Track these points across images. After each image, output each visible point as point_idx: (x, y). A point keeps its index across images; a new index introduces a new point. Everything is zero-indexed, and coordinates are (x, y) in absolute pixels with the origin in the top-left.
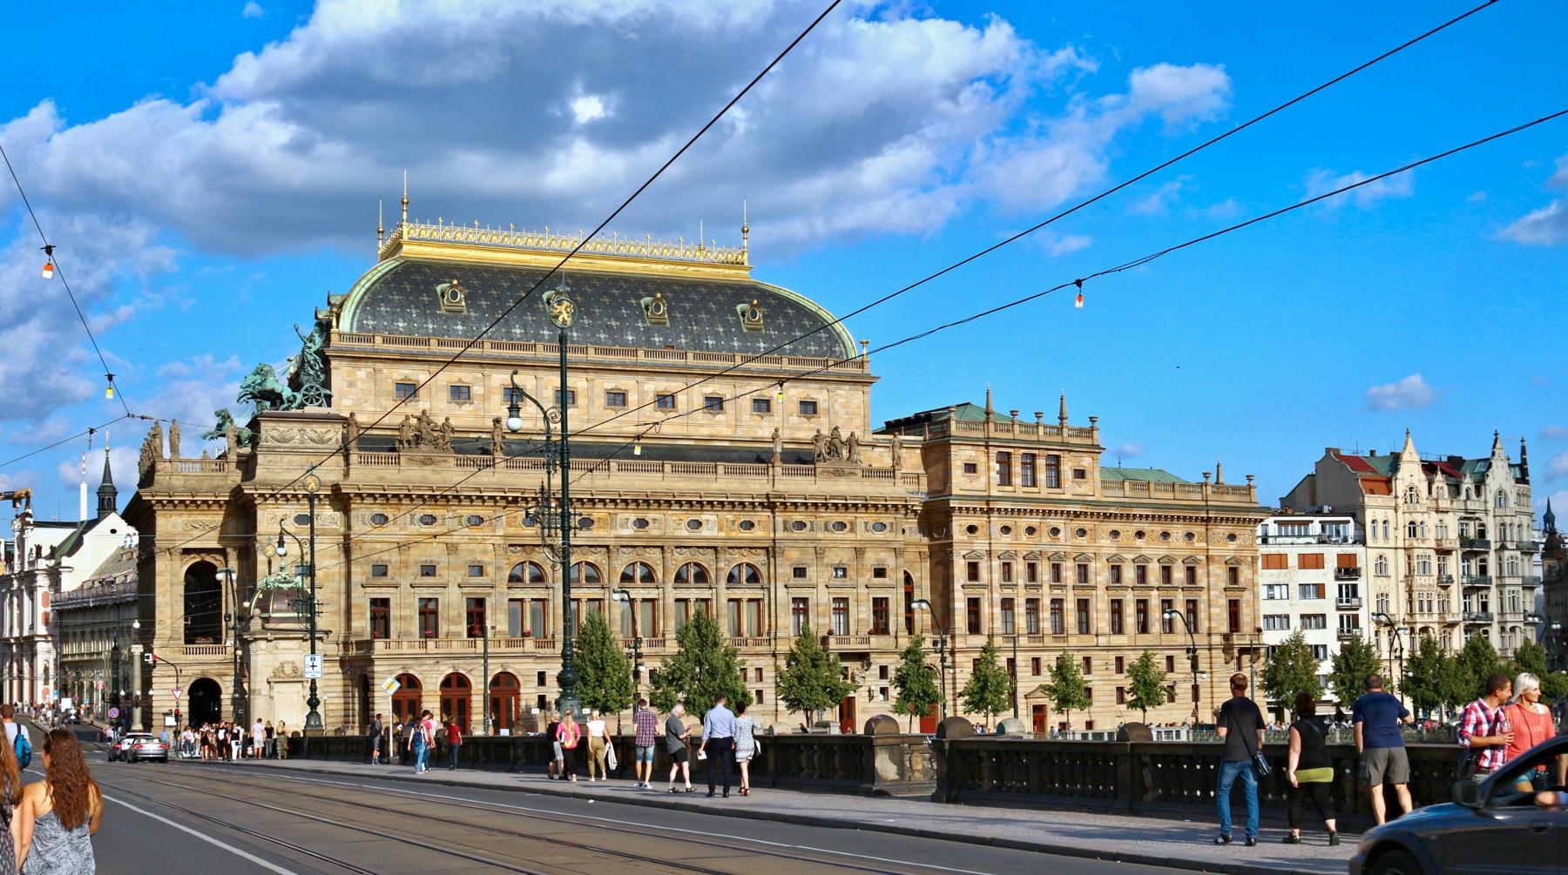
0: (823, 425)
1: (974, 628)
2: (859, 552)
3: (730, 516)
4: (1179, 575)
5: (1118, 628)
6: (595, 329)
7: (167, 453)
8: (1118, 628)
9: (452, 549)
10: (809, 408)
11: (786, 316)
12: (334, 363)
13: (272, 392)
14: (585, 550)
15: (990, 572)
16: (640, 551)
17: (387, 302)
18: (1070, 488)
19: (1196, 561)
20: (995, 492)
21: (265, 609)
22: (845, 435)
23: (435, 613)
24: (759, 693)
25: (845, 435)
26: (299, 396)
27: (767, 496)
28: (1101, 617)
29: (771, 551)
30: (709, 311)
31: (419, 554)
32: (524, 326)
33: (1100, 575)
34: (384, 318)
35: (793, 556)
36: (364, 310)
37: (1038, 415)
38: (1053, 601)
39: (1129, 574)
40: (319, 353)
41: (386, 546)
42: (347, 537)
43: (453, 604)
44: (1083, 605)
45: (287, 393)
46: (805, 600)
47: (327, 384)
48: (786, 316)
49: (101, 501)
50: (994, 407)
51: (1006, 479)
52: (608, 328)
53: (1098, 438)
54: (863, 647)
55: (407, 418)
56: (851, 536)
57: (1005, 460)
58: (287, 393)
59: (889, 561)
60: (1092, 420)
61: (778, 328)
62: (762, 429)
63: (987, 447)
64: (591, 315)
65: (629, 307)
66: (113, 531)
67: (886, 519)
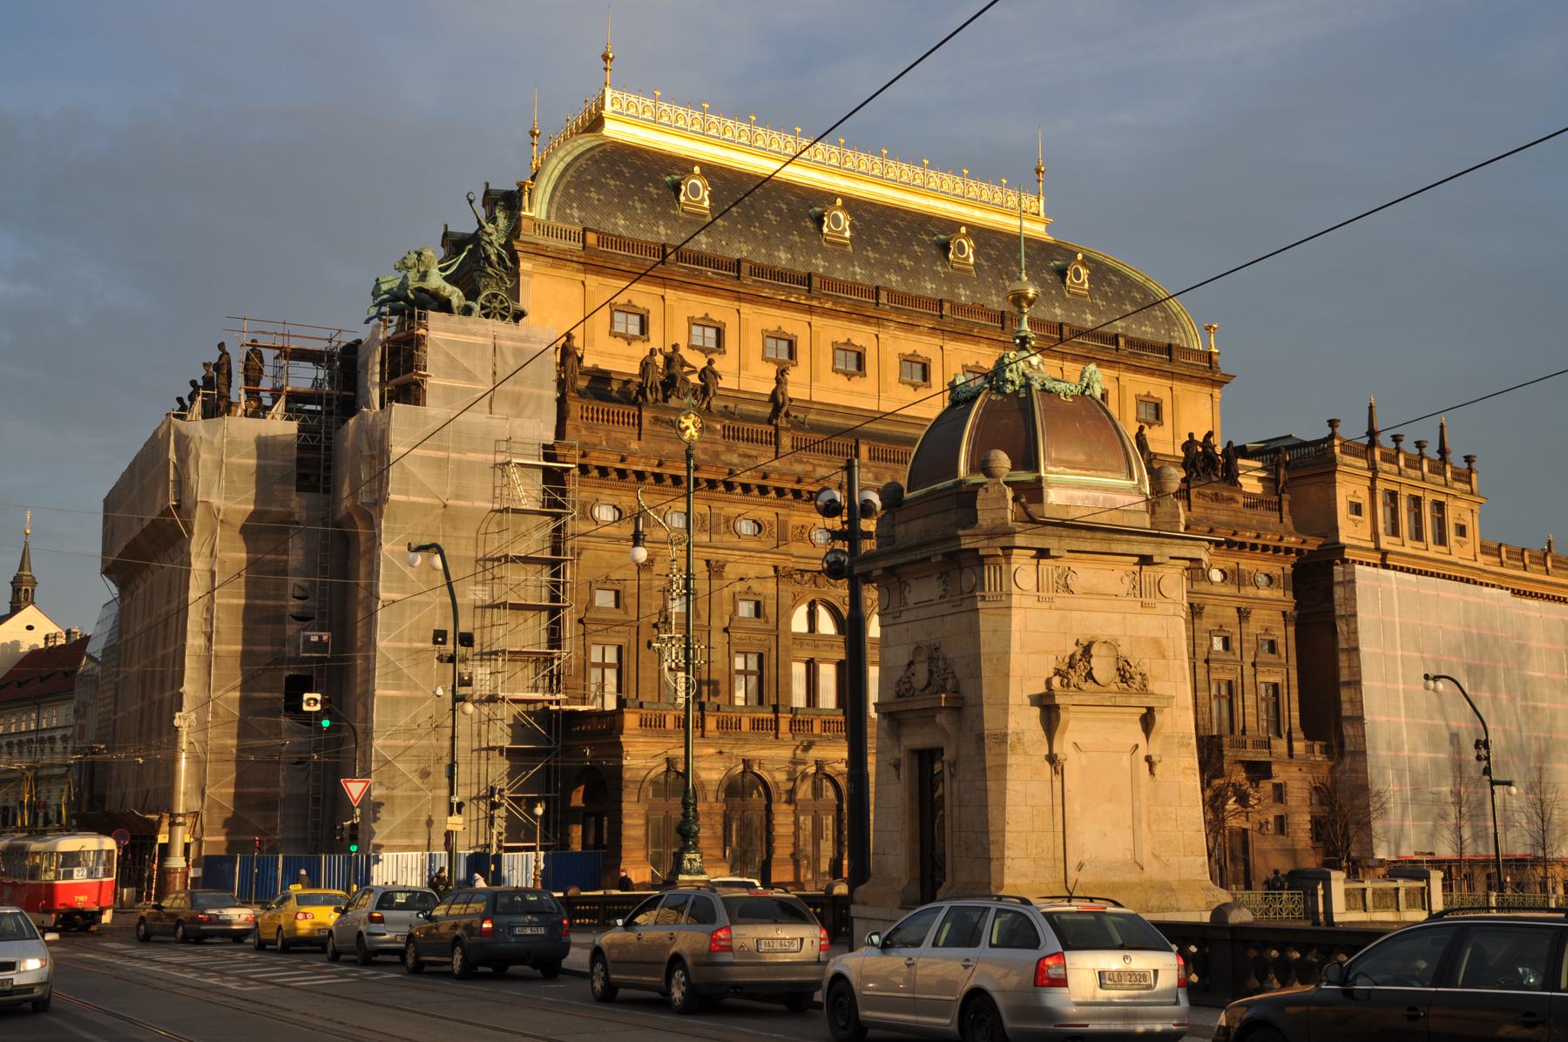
2: (1243, 614)
6: (887, 267)
11: (1110, 283)
12: (525, 265)
17: (601, 187)
21: (1027, 458)
22: (1219, 450)
26: (477, 307)
32: (791, 248)
34: (595, 208)
36: (566, 194)
45: (456, 295)
47: (515, 293)
48: (1110, 283)
50: (1378, 426)
52: (900, 269)
54: (1262, 756)
61: (1105, 297)
64: (876, 247)
65: (922, 243)
66: (30, 628)
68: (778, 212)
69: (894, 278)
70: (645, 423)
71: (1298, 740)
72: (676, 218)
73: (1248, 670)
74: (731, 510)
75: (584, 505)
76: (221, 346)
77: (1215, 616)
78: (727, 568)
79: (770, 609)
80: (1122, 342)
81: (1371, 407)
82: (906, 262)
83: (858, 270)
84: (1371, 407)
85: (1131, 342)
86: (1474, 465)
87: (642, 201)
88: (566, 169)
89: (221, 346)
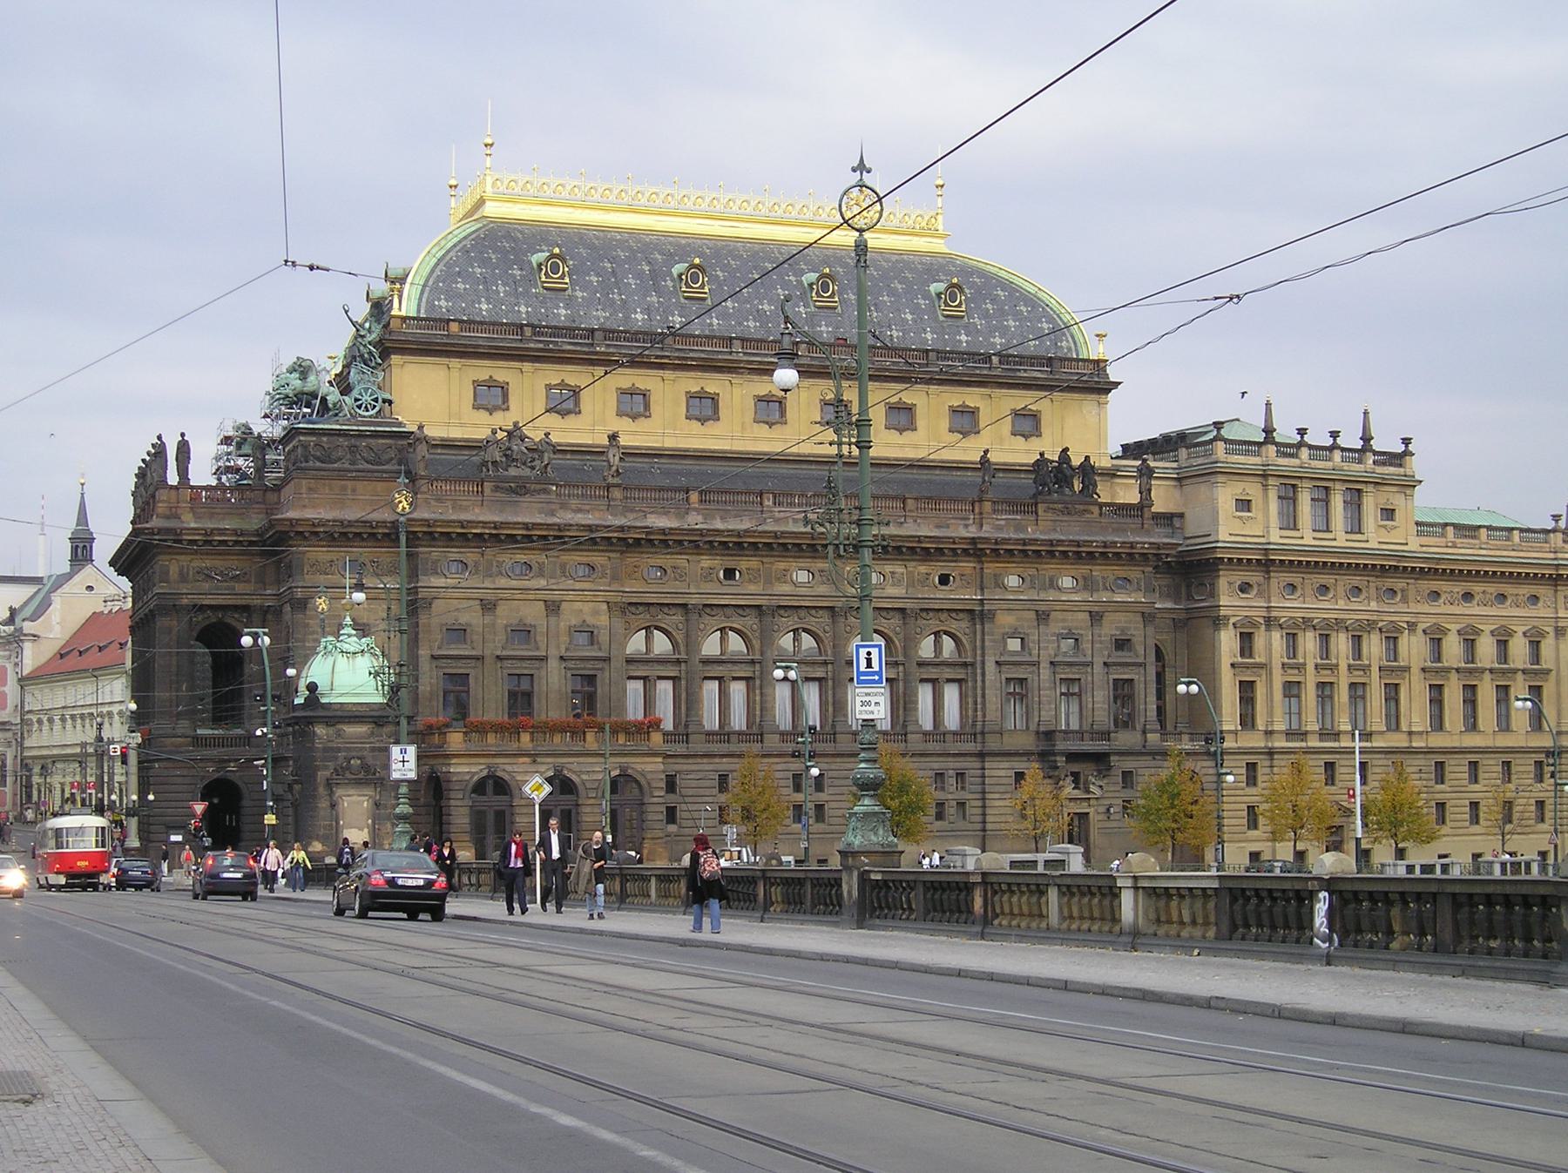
0: (1048, 446)
1: (1247, 721)
2: (1095, 618)
3: (923, 569)
4: (1519, 649)
5: (1438, 723)
7: (173, 478)
8: (1438, 723)
9: (553, 608)
10: (1027, 424)
13: (314, 395)
14: (729, 611)
15: (1271, 645)
16: (803, 613)
18: (1375, 537)
19: (1543, 634)
20: (1275, 536)
22: (1076, 461)
23: (528, 695)
24: (961, 805)
25: (1076, 461)
27: (973, 541)
28: (1415, 712)
29: (978, 615)
30: (892, 292)
31: (506, 615)
32: (647, 310)
33: (1413, 649)
35: (1005, 620)
37: (1334, 435)
38: (1353, 685)
39: (1453, 649)
40: (379, 344)
41: (465, 604)
42: (413, 591)
43: (553, 682)
44: (1392, 693)
46: (1022, 681)
49: (75, 550)
51: (1290, 522)
53: (1416, 466)
55: (494, 432)
56: (1086, 596)
57: (1289, 497)
58: (334, 396)
59: (1136, 630)
60: (1406, 441)
62: (968, 451)
63: (1265, 476)
67: (1134, 573)
68: (639, 275)
69: (751, 324)
70: (487, 491)
71: (1153, 731)
72: (536, 296)
73: (1098, 668)
74: (565, 558)
75: (435, 562)
76: (159, 438)
77: (1064, 620)
78: (564, 605)
79: (604, 638)
80: (995, 359)
81: (1268, 404)
82: (766, 307)
83: (715, 321)
84: (1268, 404)
85: (1004, 357)
86: (1411, 447)
87: (504, 285)
88: (437, 264)
89: (159, 438)
